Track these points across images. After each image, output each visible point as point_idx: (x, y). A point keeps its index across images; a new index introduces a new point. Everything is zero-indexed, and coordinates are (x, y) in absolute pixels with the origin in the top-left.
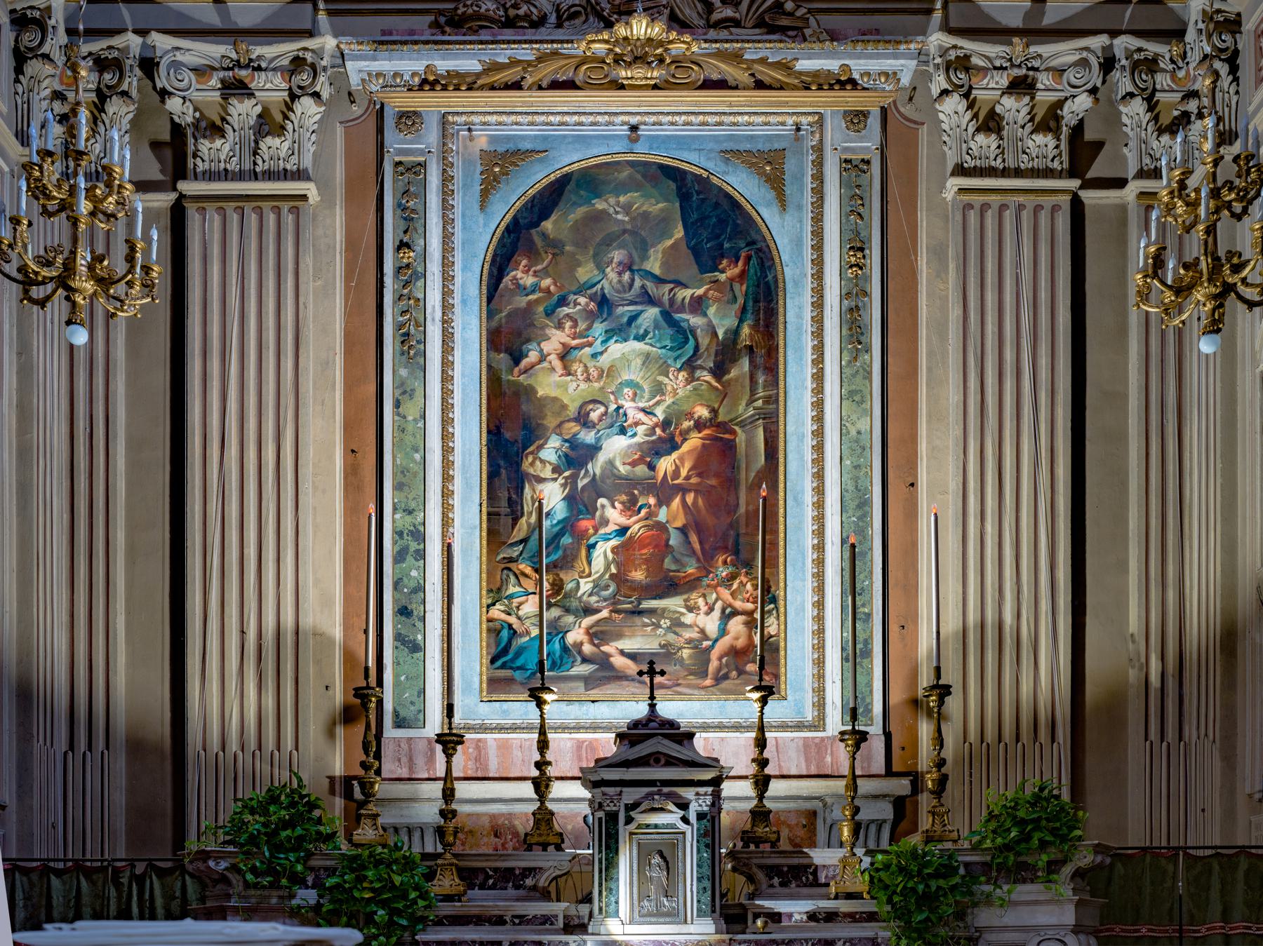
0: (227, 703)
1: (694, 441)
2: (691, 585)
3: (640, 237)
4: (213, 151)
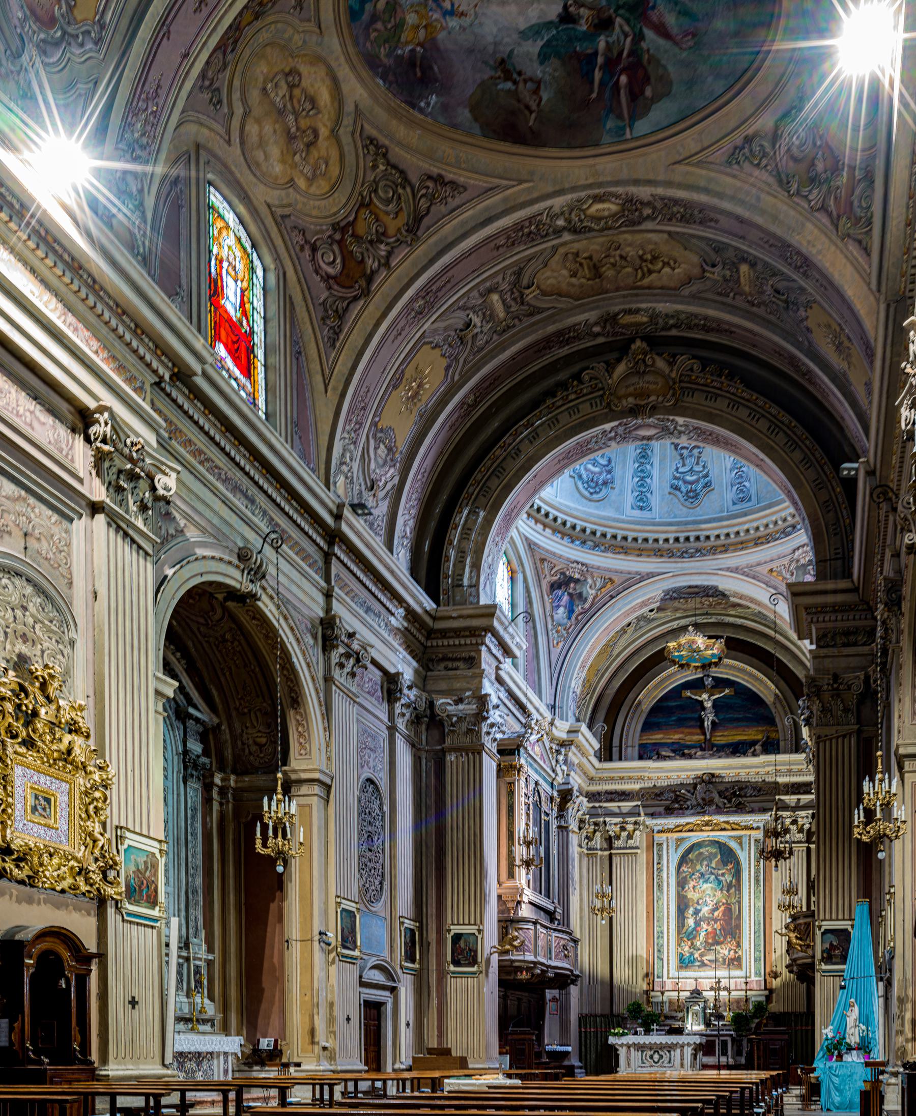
0: (621, 974)
1: (722, 908)
2: (722, 943)
3: (710, 858)
4: (617, 843)
